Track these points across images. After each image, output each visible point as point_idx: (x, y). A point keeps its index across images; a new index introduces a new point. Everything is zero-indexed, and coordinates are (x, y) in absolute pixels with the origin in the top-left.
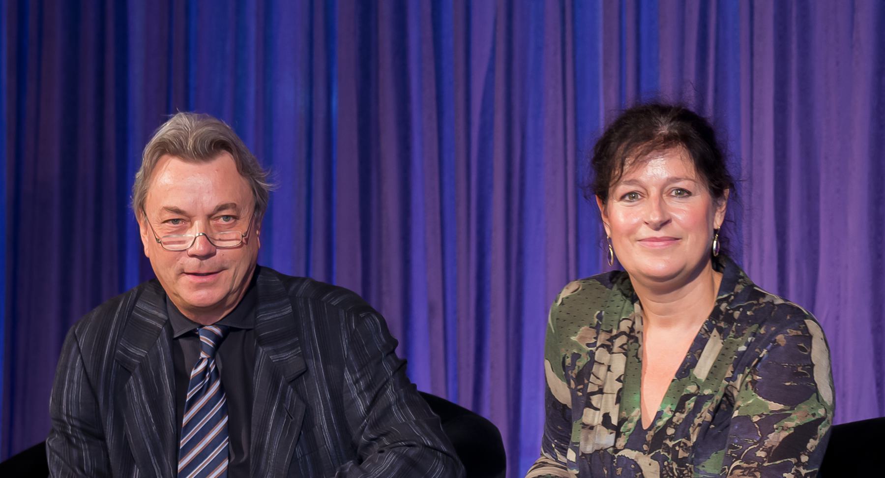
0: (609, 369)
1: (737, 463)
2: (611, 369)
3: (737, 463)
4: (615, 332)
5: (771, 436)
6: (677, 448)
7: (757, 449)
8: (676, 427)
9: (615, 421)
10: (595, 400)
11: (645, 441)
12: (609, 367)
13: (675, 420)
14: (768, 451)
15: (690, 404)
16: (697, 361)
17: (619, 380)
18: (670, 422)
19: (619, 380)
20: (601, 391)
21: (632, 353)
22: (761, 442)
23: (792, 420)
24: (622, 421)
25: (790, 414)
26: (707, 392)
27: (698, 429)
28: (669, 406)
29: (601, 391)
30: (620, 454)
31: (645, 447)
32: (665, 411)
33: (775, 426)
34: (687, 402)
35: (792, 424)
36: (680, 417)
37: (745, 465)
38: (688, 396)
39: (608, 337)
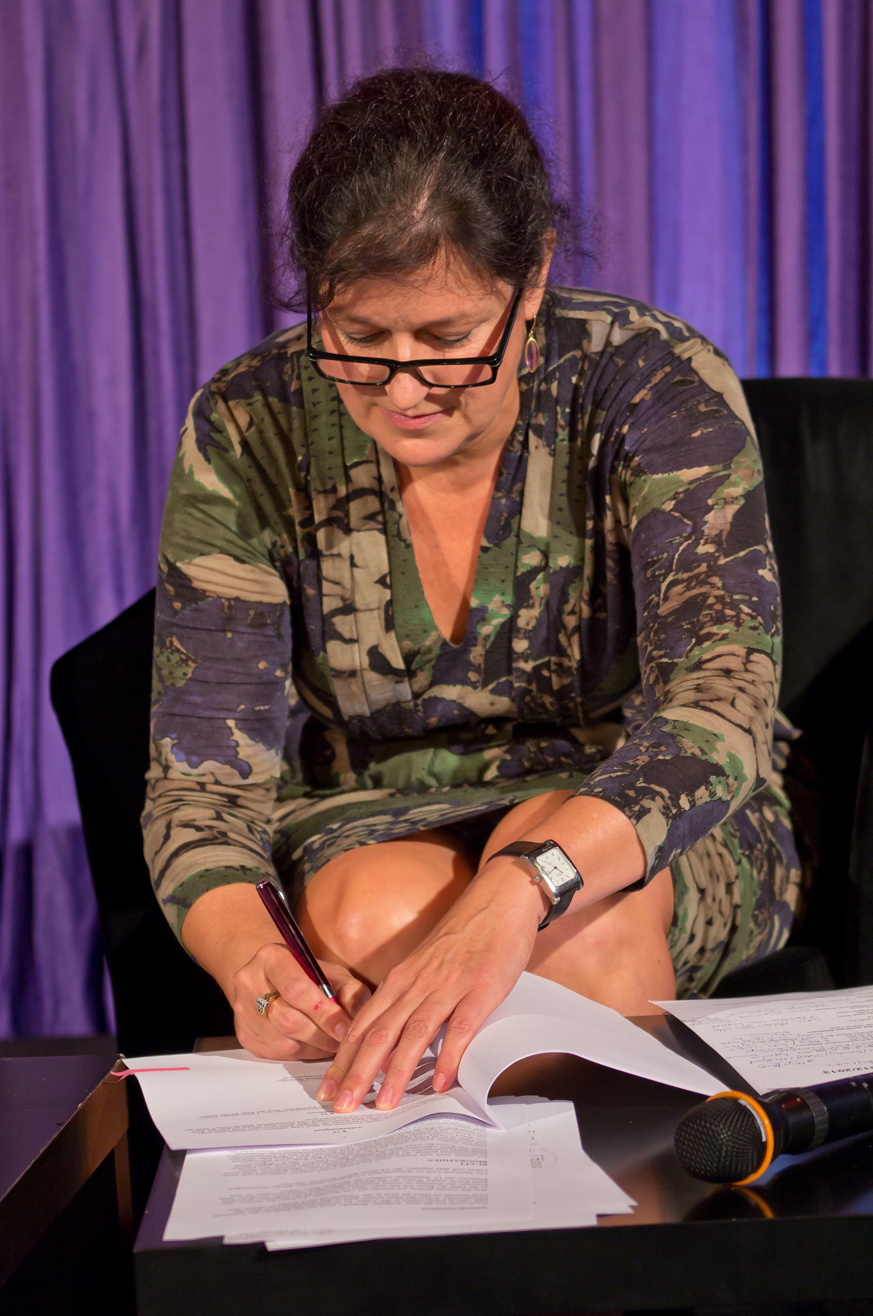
0: (353, 565)
1: (670, 578)
2: (357, 560)
3: (670, 578)
4: (342, 491)
5: (710, 517)
6: (546, 673)
7: (696, 543)
8: (529, 635)
9: (398, 662)
10: (343, 624)
11: (469, 666)
12: (352, 557)
13: (521, 622)
14: (717, 540)
15: (539, 588)
16: (521, 504)
17: (382, 581)
18: (509, 629)
19: (382, 581)
20: (348, 609)
21: (392, 529)
22: (697, 532)
23: (735, 484)
24: (408, 658)
25: (729, 476)
26: (563, 561)
27: (575, 639)
28: (498, 598)
29: (348, 609)
30: (426, 696)
31: (473, 676)
32: (491, 607)
33: (710, 502)
34: (533, 585)
35: (737, 491)
36: (527, 617)
37: (685, 576)
38: (533, 573)
39: (332, 500)
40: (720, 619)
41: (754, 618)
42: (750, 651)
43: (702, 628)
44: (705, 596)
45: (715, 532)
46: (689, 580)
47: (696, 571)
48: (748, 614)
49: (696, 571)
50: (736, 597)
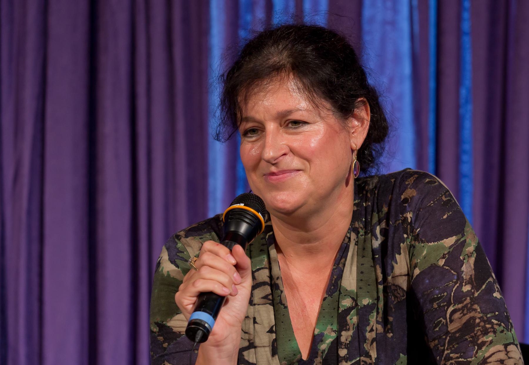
40: (485, 332)
41: (500, 325)
42: (506, 346)
43: (478, 339)
44: (474, 318)
45: (468, 277)
46: (462, 309)
47: (465, 303)
48: (497, 324)
49: (465, 303)
50: (489, 316)
